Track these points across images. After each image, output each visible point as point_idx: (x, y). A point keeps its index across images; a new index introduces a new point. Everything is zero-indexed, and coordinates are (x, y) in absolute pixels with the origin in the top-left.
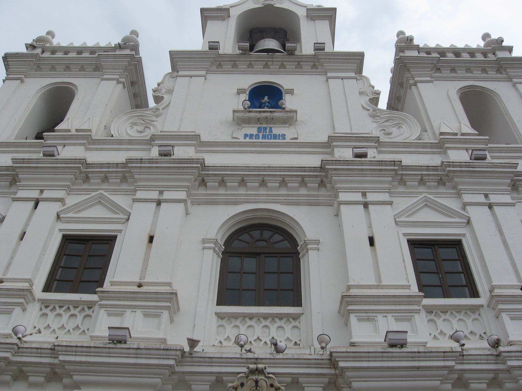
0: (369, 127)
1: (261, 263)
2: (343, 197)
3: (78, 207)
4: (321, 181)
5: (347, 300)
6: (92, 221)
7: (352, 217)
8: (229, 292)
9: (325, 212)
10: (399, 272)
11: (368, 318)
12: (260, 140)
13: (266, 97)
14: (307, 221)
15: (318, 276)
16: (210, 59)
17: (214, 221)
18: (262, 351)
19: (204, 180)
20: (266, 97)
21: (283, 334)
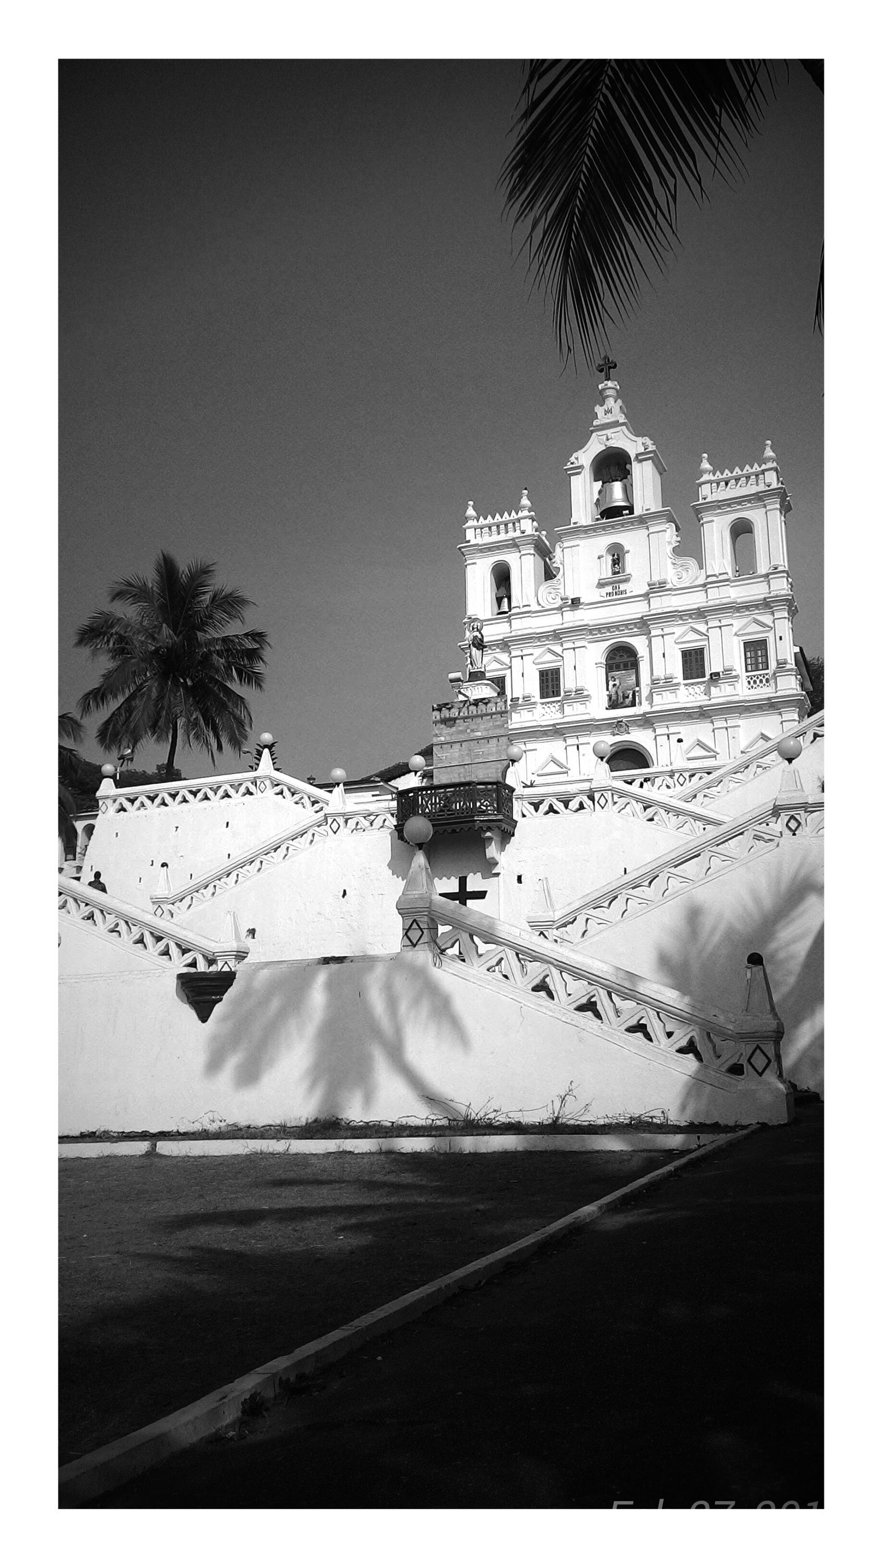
2: (653, 633)
4: (643, 625)
10: (676, 667)
12: (615, 597)
14: (639, 643)
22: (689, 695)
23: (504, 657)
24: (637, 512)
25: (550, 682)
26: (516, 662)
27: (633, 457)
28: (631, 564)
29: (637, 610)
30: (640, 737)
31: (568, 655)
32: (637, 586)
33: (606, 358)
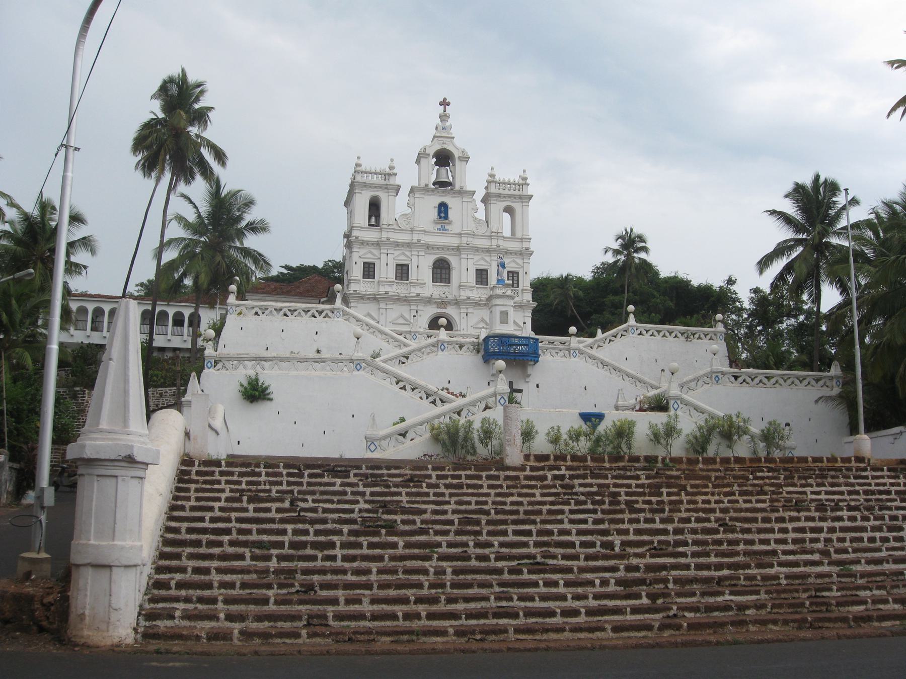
0: (470, 227)
1: (442, 271)
2: (463, 256)
3: (398, 256)
4: (458, 249)
5: (460, 286)
6: (403, 260)
7: (464, 261)
8: (434, 280)
9: (457, 258)
10: (472, 278)
11: (464, 290)
13: (443, 209)
14: (453, 260)
15: (454, 275)
16: (425, 190)
17: (430, 260)
18: (444, 296)
19: (428, 247)
20: (443, 209)
21: (446, 289)
22: (480, 293)
23: (376, 252)
24: (457, 187)
25: (402, 271)
26: (384, 256)
27: (456, 156)
28: (451, 214)
29: (453, 241)
30: (451, 311)
31: (414, 258)
32: (455, 228)
33: (445, 99)
